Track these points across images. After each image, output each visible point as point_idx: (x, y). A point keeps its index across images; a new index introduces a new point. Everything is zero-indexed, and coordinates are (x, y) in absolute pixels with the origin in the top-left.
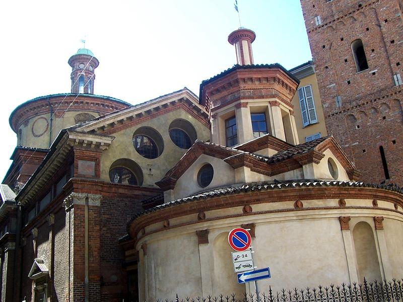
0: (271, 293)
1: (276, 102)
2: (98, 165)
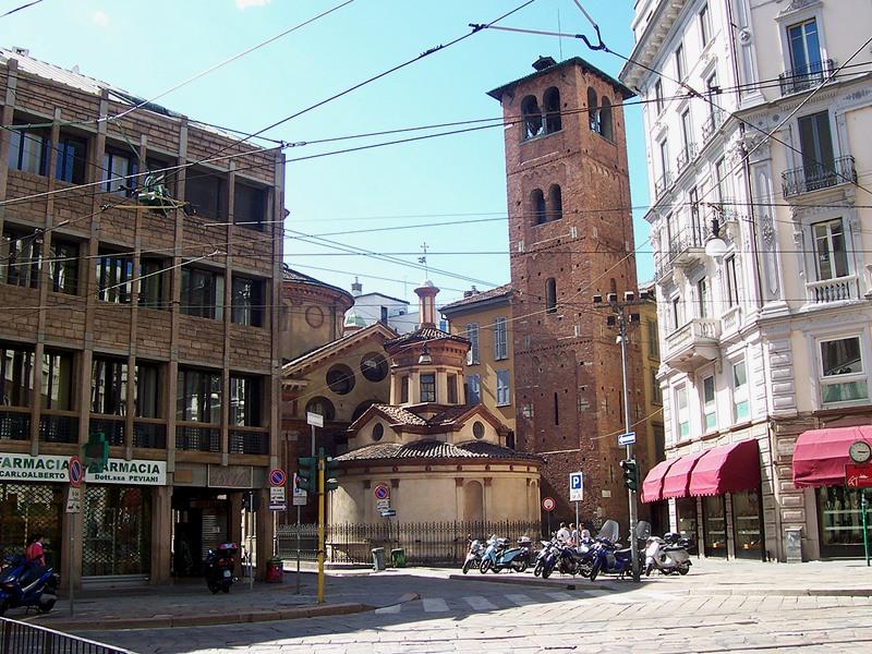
2: (295, 403)
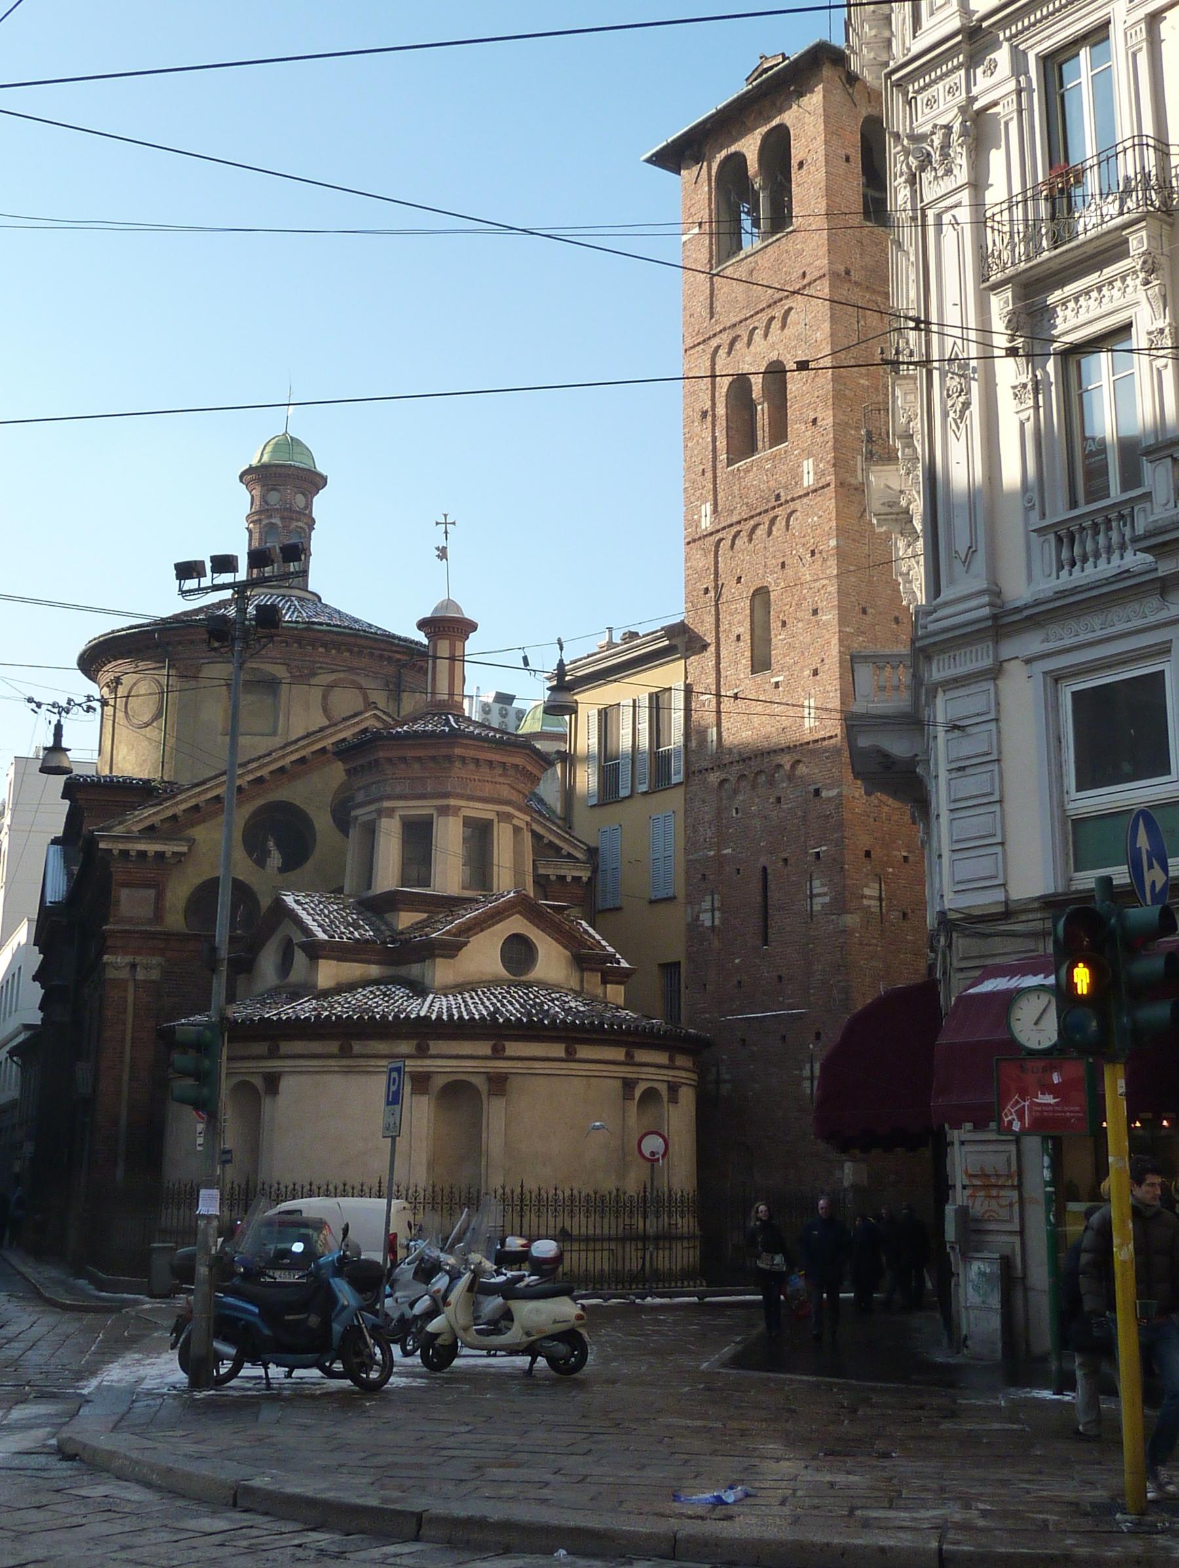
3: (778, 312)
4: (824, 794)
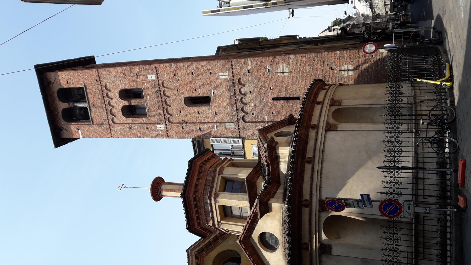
0: (384, 193)
1: (220, 169)
3: (105, 93)
4: (250, 67)
